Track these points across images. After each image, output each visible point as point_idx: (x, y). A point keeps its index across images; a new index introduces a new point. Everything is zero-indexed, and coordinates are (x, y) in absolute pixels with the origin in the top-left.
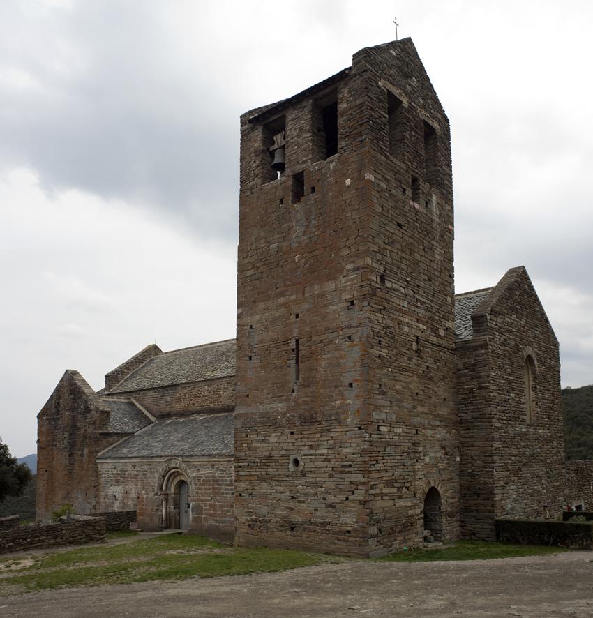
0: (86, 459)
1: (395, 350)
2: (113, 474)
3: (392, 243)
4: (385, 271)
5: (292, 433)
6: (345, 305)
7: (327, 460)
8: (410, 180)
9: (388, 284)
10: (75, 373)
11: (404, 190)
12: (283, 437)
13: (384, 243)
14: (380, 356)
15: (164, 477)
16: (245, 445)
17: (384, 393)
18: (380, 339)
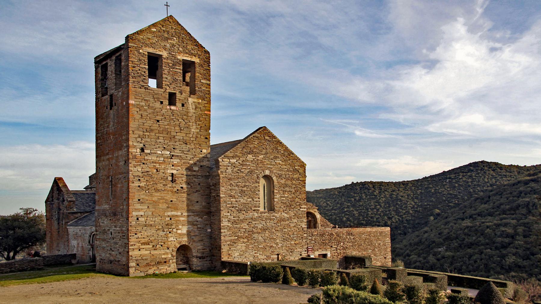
0: (64, 226)
1: (152, 182)
2: (73, 234)
3: (152, 130)
4: (144, 146)
5: (110, 220)
6: (124, 162)
7: (119, 233)
8: (167, 96)
9: (146, 151)
10: (61, 179)
11: (162, 103)
12: (108, 222)
13: (143, 132)
14: (139, 186)
15: (90, 236)
16: (98, 224)
17: (142, 203)
18: (139, 178)
